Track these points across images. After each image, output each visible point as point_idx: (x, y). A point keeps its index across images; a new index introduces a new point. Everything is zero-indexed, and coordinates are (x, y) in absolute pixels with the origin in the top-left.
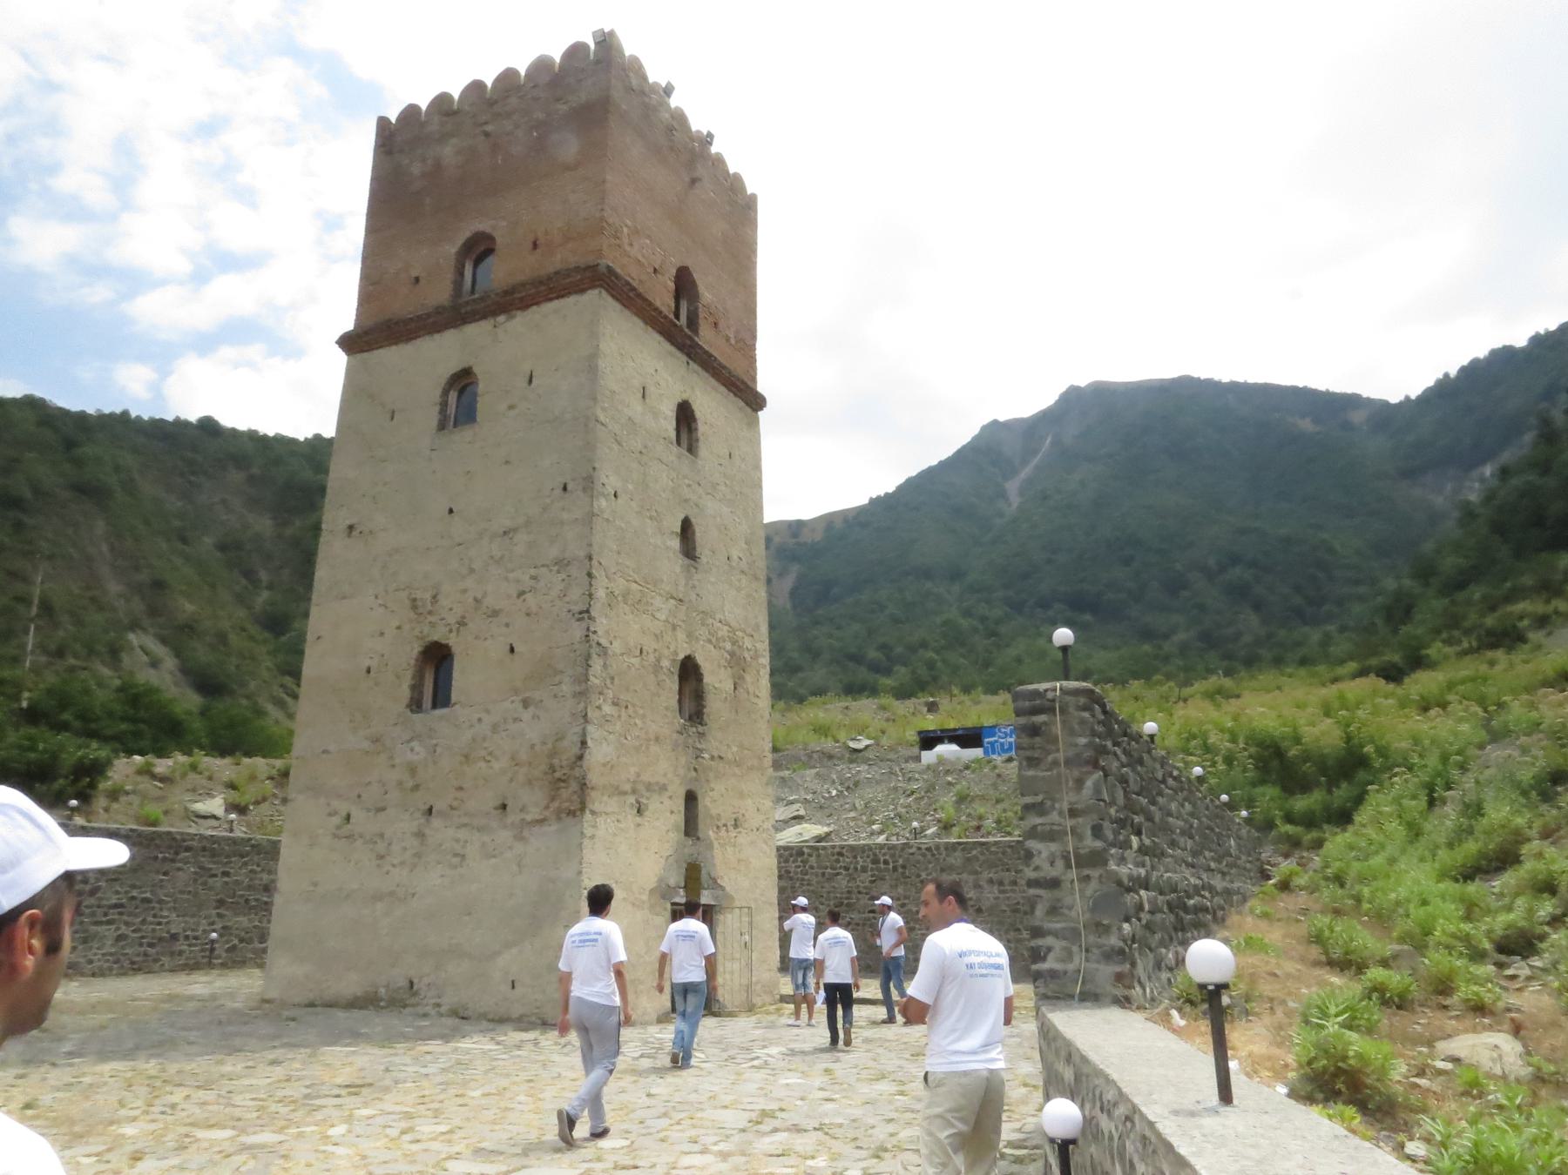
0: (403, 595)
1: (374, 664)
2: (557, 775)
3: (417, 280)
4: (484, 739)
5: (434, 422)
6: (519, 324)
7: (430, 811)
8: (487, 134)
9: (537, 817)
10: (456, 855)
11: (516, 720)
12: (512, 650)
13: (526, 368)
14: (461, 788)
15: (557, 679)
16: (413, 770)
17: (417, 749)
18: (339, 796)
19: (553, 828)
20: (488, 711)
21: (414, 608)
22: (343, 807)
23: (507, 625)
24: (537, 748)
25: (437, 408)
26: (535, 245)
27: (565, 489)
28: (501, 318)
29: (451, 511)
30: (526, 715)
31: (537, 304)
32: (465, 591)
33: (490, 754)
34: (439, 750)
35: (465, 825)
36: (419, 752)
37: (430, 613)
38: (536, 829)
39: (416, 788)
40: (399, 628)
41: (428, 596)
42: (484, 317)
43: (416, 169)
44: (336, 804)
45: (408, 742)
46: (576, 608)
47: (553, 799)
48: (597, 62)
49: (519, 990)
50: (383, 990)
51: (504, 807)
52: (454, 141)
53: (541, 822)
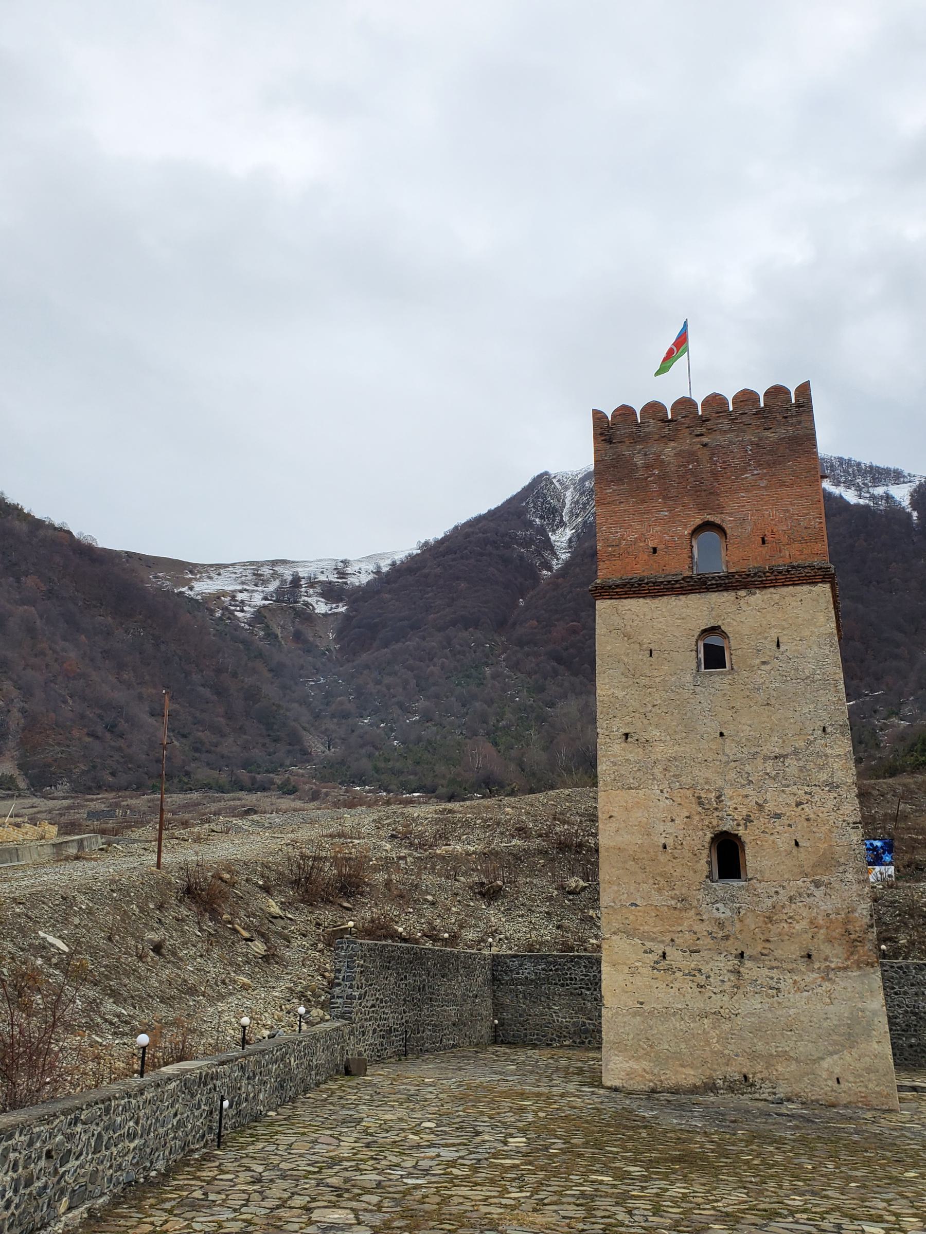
0: (689, 793)
1: (670, 842)
2: (852, 937)
3: (655, 550)
4: (783, 907)
5: (694, 666)
6: (759, 598)
7: (742, 955)
8: (705, 445)
9: (840, 965)
10: (771, 988)
11: (809, 895)
12: (797, 844)
13: (774, 634)
14: (768, 941)
15: (841, 869)
16: (721, 924)
17: (722, 910)
18: (653, 940)
19: (857, 973)
20: (784, 887)
21: (700, 804)
22: (659, 949)
23: (790, 825)
24: (833, 916)
25: (694, 653)
26: (764, 542)
27: (824, 730)
28: (742, 593)
29: (722, 734)
30: (819, 893)
31: (774, 587)
32: (747, 796)
33: (791, 918)
34: (743, 912)
35: (777, 968)
36: (724, 912)
37: (716, 809)
38: (840, 974)
39: (727, 938)
40: (687, 817)
41: (712, 796)
42: (727, 590)
43: (639, 461)
44: (649, 945)
45: (713, 903)
46: (851, 820)
47: (852, 954)
48: (798, 405)
49: (844, 1085)
50: (721, 1082)
51: (809, 956)
52: (673, 444)
53: (845, 969)
